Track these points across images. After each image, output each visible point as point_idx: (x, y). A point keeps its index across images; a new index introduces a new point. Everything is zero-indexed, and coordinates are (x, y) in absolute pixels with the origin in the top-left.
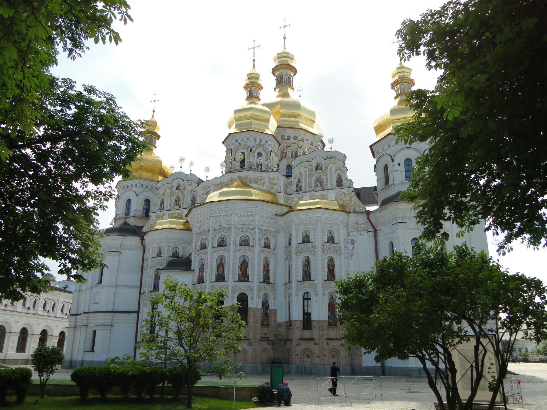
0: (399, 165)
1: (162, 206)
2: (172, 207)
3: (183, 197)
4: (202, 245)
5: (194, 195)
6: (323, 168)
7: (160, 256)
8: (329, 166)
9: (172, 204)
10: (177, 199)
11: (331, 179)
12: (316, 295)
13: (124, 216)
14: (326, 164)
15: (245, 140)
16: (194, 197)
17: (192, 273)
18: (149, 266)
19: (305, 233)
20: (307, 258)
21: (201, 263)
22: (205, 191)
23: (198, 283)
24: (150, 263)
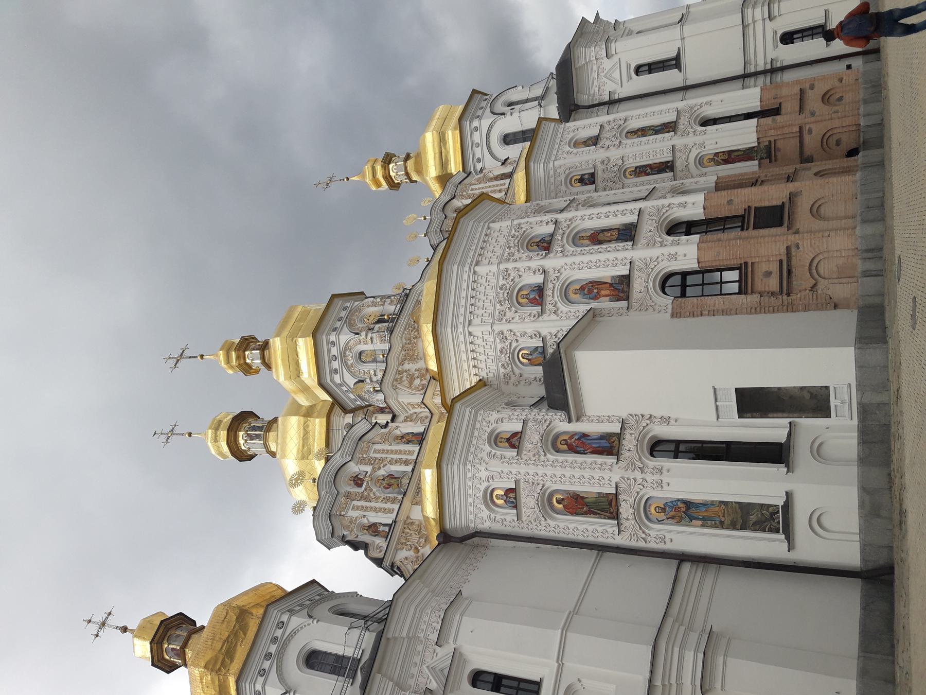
0: (514, 109)
1: (381, 528)
2: (400, 497)
3: (391, 462)
7: (520, 438)
9: (392, 496)
11: (494, 186)
12: (709, 103)
15: (343, 314)
16: (402, 437)
17: (598, 319)
20: (629, 134)
21: (577, 297)
22: (406, 383)
23: (627, 299)
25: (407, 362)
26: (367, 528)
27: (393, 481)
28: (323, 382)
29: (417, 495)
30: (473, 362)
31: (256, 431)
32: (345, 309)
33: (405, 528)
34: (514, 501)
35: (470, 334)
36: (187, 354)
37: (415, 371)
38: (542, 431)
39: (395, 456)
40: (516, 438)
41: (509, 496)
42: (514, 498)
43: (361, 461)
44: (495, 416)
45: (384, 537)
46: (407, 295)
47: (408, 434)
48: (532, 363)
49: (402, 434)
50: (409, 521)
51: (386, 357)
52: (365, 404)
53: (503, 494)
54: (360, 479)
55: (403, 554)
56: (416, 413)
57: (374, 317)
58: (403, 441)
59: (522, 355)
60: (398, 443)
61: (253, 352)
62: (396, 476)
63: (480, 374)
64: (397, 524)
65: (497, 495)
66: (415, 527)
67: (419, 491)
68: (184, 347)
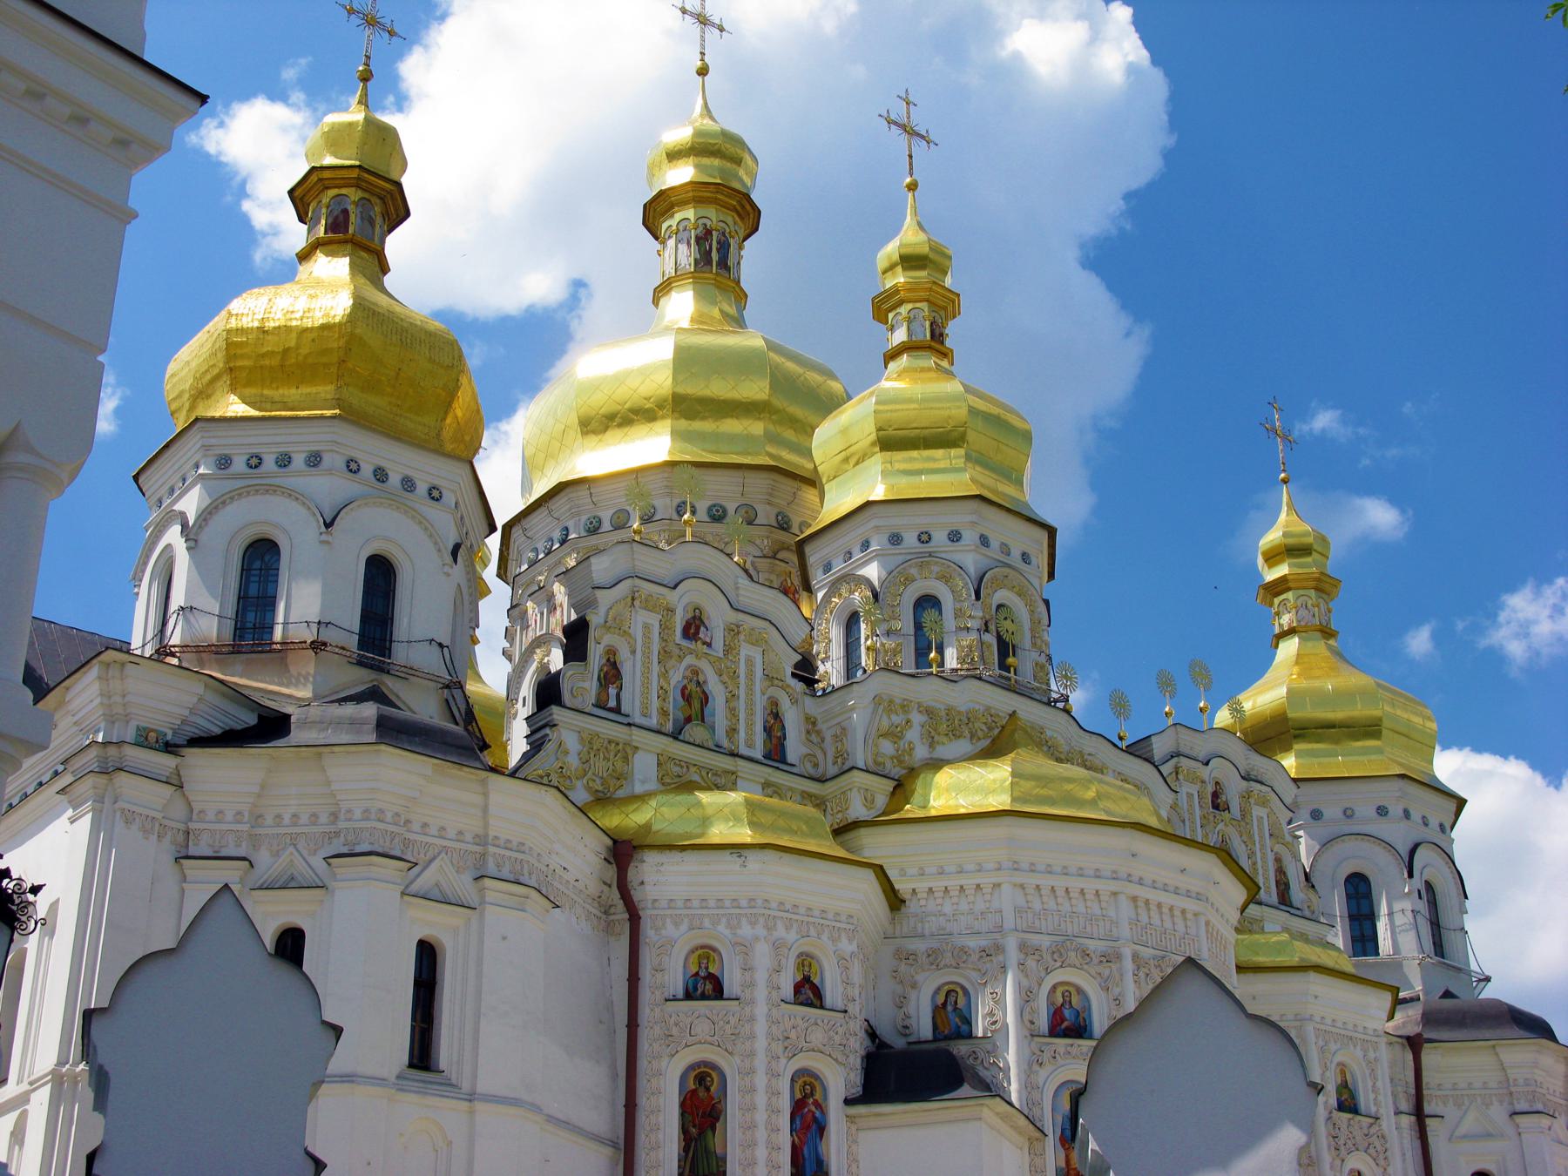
0: (1420, 897)
1: (612, 691)
2: (669, 727)
3: (732, 697)
4: (1056, 1017)
5: (774, 703)
6: (1235, 810)
7: (811, 1005)
8: (1258, 812)
10: (692, 687)
13: (353, 642)
14: (1246, 796)
18: (761, 1044)
19: (1338, 1071)
22: (885, 724)
24: (761, 1027)
25: (923, 718)
26: (612, 660)
27: (696, 704)
28: (875, 509)
29: (675, 763)
30: (940, 889)
31: (718, 250)
32: (1025, 558)
33: (618, 744)
34: (699, 992)
35: (997, 886)
36: (919, 148)
37: (910, 743)
38: (827, 1050)
39: (742, 705)
40: (811, 996)
41: (707, 983)
42: (703, 993)
43: (733, 630)
44: (847, 947)
45: (599, 695)
46: (1049, 703)
47: (783, 727)
48: (938, 1011)
49: (783, 715)
50: (628, 750)
51: (931, 674)
52: (820, 589)
53: (711, 970)
54: (697, 632)
55: (571, 741)
56: (823, 741)
57: (1010, 632)
58: (769, 719)
59: (957, 992)
60: (765, 708)
61: (927, 324)
62: (707, 711)
63: (914, 901)
64: (625, 729)
65: (708, 958)
66: (619, 764)
67: (682, 767)
68: (932, 137)
